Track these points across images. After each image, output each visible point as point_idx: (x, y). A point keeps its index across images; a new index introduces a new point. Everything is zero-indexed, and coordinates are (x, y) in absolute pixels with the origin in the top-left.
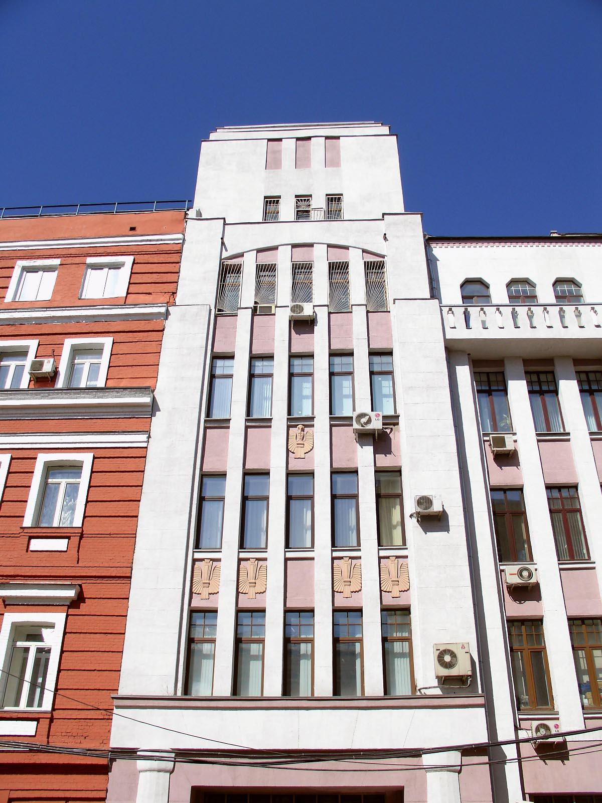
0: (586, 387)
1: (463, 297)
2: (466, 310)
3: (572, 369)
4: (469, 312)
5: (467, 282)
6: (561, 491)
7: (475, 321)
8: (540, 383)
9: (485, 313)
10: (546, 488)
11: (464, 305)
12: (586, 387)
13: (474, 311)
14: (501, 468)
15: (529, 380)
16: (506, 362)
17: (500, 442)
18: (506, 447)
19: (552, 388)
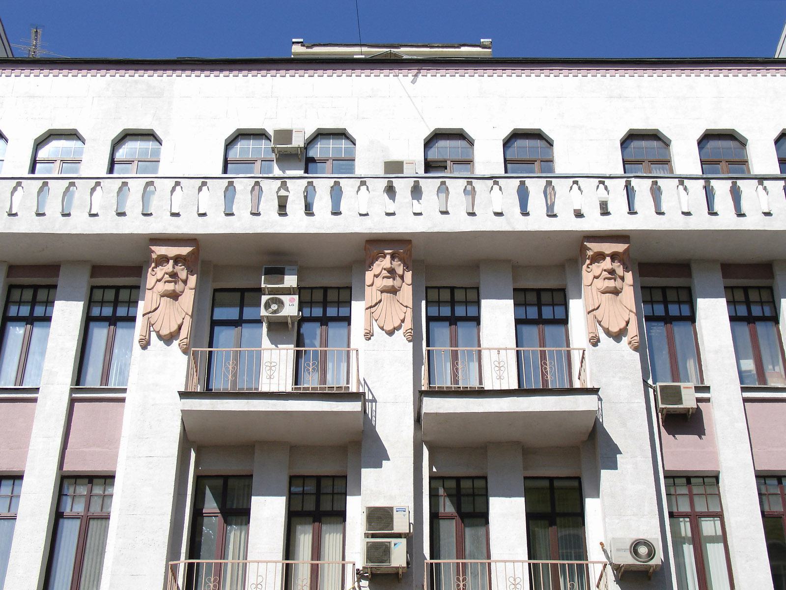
0: (742, 311)
1: (625, 162)
2: (734, 184)
3: (719, 281)
4: (712, 187)
5: (632, 136)
6: (782, 483)
7: (536, 202)
8: (748, 303)
9: (606, 188)
10: (756, 477)
11: (627, 175)
12: (742, 311)
13: (722, 188)
14: (674, 437)
15: (731, 299)
16: (694, 267)
17: (672, 394)
18: (682, 403)
19: (768, 312)
